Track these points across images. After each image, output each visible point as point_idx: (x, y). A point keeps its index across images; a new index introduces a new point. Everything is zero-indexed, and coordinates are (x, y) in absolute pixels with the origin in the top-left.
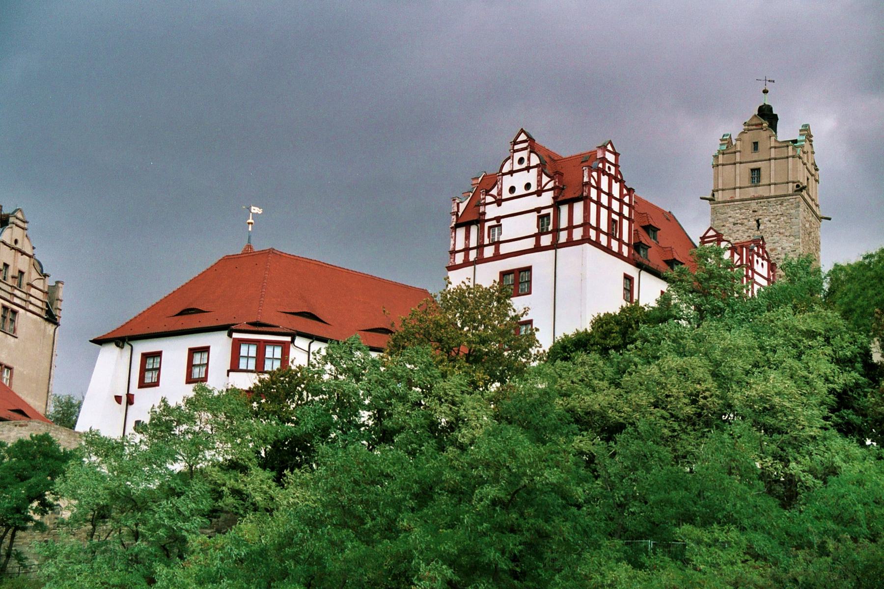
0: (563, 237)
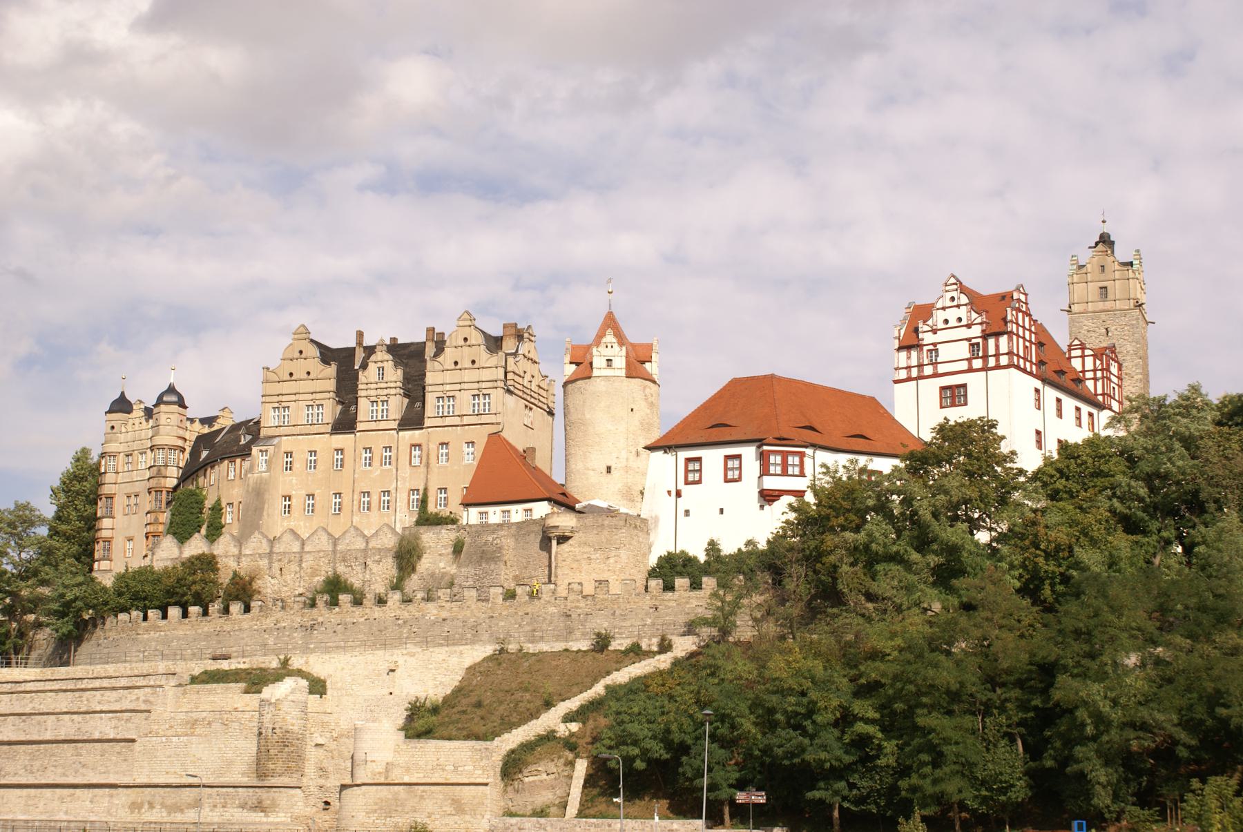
0: (992, 362)
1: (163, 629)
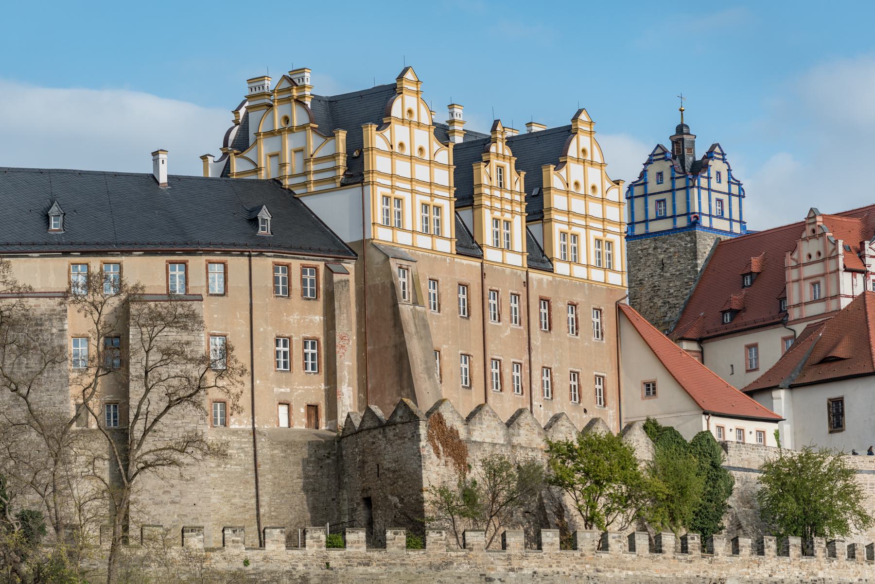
1: (630, 566)
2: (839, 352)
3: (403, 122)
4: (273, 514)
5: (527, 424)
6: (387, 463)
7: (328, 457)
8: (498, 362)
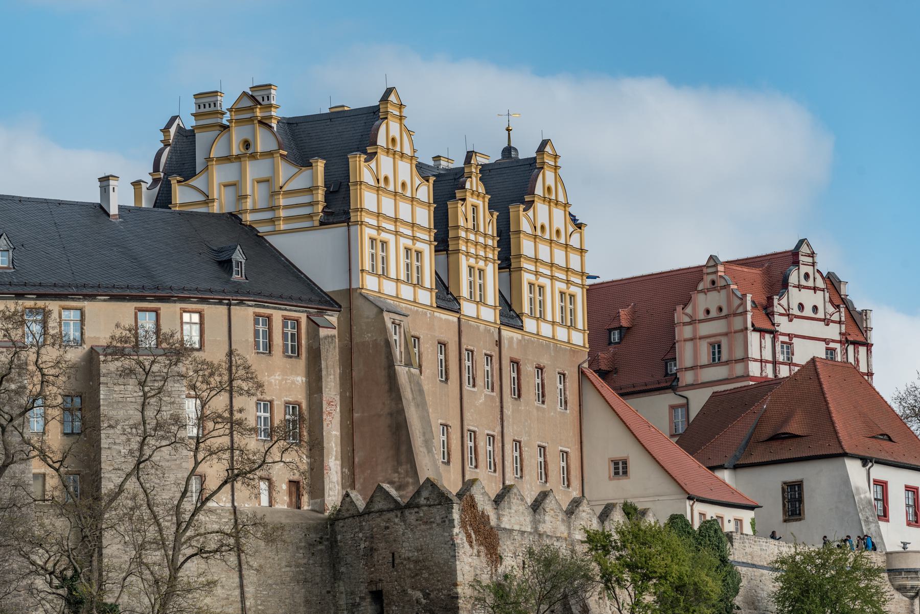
2: (793, 427)
3: (388, 153)
4: (260, 607)
5: (552, 510)
6: (406, 550)
7: (320, 543)
8: (473, 434)
